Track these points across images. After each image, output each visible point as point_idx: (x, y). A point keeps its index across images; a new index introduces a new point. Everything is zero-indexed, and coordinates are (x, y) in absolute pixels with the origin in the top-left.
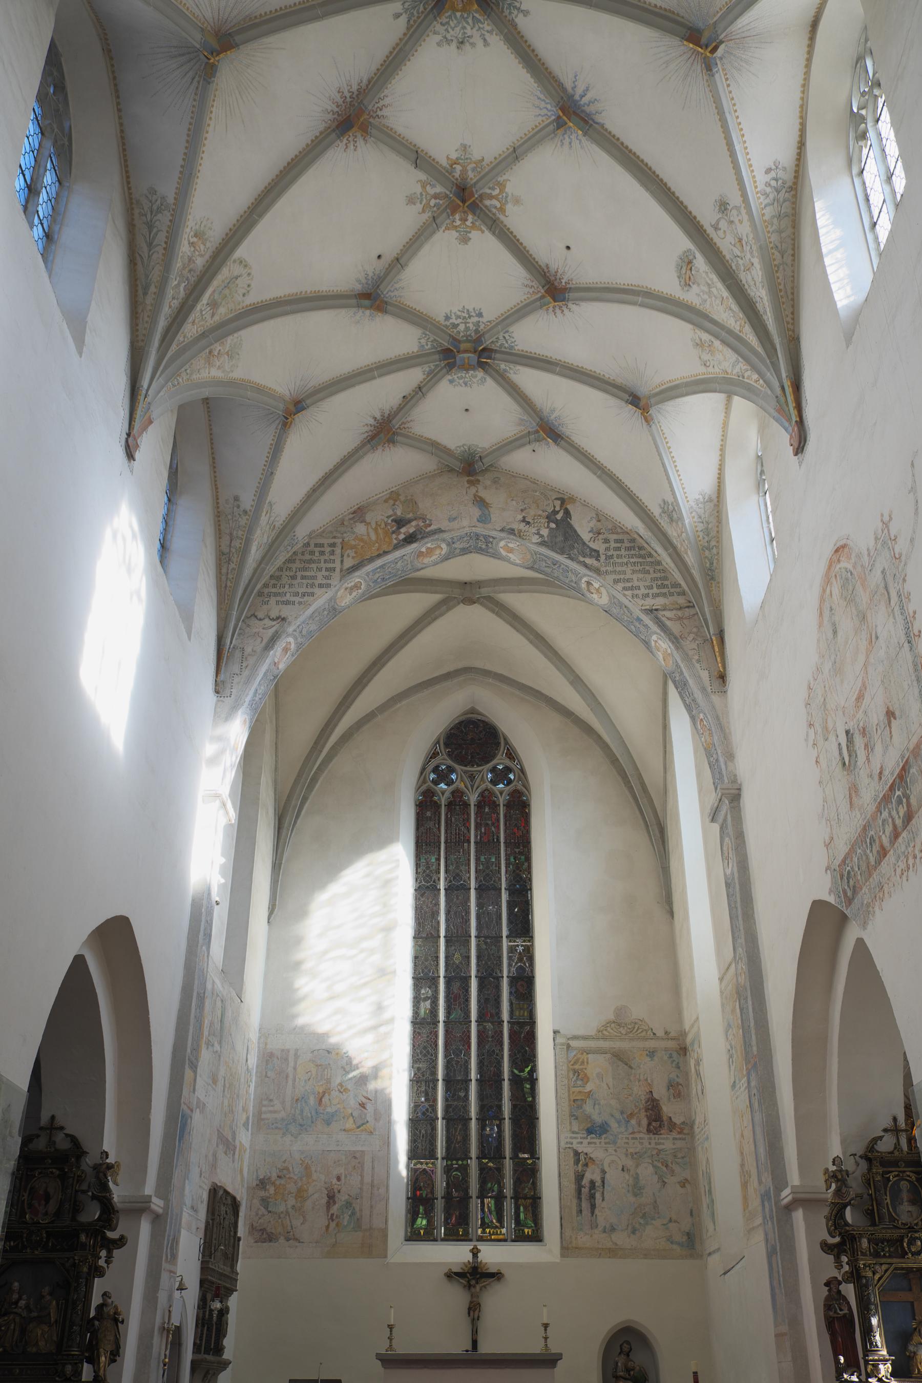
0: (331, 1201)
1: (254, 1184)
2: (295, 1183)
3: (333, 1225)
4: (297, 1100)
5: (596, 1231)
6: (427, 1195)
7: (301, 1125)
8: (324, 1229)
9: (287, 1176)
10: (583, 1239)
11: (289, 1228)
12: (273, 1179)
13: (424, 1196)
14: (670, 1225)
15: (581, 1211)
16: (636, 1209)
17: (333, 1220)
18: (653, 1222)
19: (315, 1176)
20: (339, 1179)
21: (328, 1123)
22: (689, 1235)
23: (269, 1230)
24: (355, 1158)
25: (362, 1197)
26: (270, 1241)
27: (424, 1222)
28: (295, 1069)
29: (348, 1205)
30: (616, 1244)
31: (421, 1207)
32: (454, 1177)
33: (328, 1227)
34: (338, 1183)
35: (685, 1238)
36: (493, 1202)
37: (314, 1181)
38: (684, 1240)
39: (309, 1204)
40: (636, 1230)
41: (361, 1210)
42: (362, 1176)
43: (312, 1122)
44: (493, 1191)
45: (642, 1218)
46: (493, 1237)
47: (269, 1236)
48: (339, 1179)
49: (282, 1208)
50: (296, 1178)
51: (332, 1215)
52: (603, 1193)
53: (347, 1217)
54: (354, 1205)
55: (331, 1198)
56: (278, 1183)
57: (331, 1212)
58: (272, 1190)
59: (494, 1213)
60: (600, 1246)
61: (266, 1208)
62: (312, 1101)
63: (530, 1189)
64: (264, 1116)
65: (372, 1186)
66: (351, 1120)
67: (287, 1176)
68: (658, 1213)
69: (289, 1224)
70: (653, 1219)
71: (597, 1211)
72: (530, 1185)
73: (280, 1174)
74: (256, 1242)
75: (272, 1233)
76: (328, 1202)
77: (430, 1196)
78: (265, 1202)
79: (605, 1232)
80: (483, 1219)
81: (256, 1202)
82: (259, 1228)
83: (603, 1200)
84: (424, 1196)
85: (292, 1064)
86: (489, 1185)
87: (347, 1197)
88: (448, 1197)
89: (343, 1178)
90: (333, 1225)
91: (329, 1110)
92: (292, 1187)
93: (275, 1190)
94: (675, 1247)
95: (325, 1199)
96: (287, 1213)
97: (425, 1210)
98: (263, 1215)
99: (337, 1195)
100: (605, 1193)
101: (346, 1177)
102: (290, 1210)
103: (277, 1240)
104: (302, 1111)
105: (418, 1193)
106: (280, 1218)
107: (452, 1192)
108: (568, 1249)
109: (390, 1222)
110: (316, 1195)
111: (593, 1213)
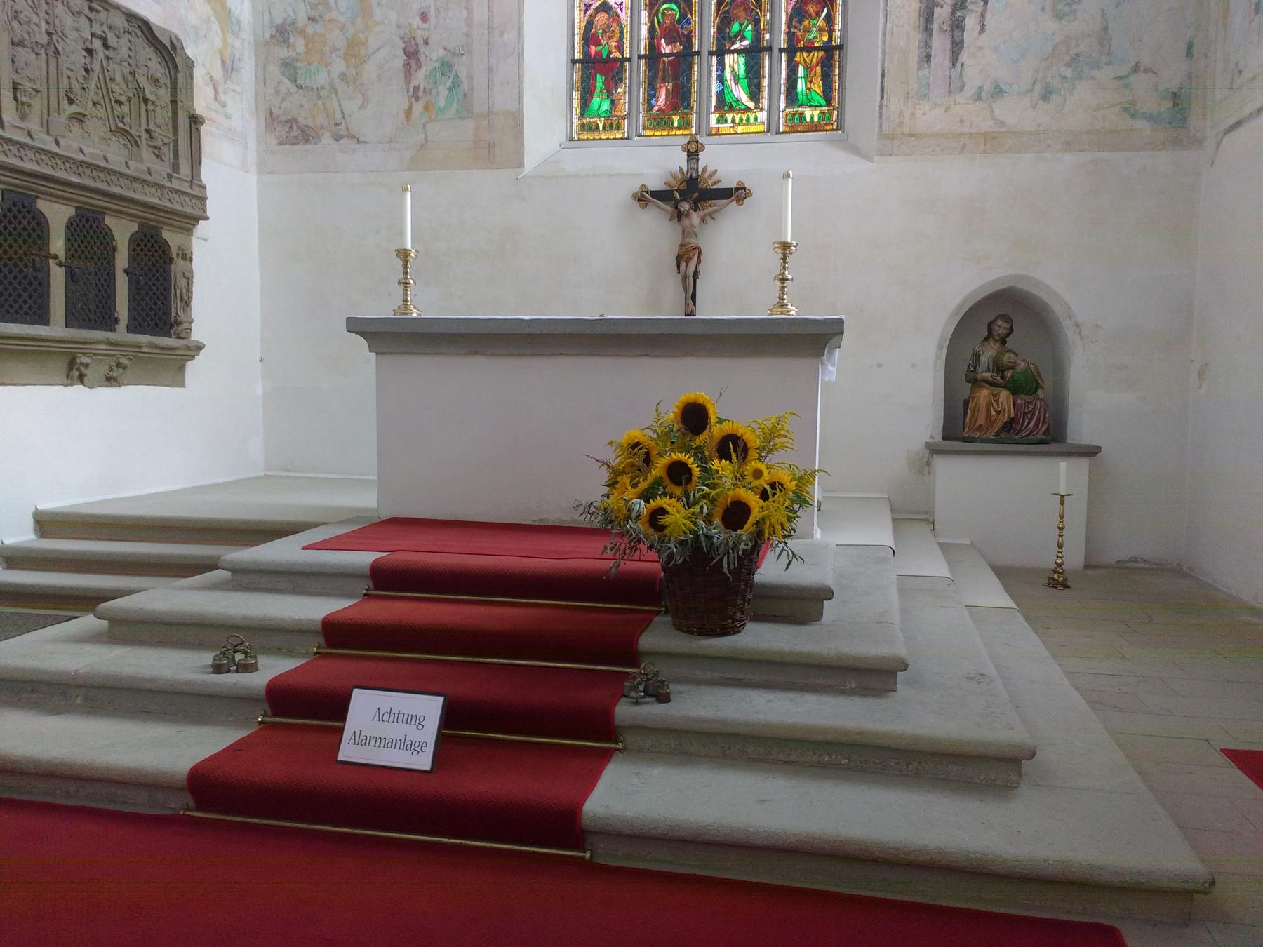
0: (413, 62)
1: (267, 36)
2: (343, 28)
3: (418, 108)
5: (960, 98)
6: (610, 53)
8: (402, 115)
9: (327, 17)
10: (930, 117)
11: (338, 116)
12: (300, 24)
13: (604, 55)
14: (1133, 78)
15: (928, 57)
16: (1055, 47)
17: (417, 99)
18: (1095, 73)
19: (378, 14)
20: (424, 17)
22: (1178, 100)
25: (471, 52)
26: (307, 141)
27: (606, 105)
29: (445, 67)
30: (1002, 123)
31: (599, 78)
32: (663, 14)
33: (409, 112)
34: (424, 26)
35: (1168, 104)
36: (742, 60)
37: (377, 24)
38: (1163, 109)
39: (370, 70)
40: (1051, 93)
41: (470, 77)
42: (469, 10)
44: (743, 38)
45: (1068, 65)
46: (740, 129)
47: (303, 131)
48: (424, 17)
49: (321, 79)
50: (342, 19)
52: (983, 16)
53: (443, 92)
54: (456, 68)
55: (412, 55)
56: (310, 30)
57: (414, 83)
58: (300, 44)
59: (745, 83)
60: (966, 129)
61: (294, 80)
63: (820, 30)
65: (490, 28)
67: (327, 17)
68: (1109, 54)
69: (338, 109)
70: (1096, 66)
71: (964, 57)
72: (821, 22)
73: (312, 14)
74: (280, 144)
75: (309, 127)
76: (407, 65)
77: (616, 54)
78: (289, 68)
79: (978, 98)
80: (720, 95)
81: (274, 70)
83: (982, 30)
84: (604, 55)
86: (736, 27)
87: (441, 52)
88: (653, 55)
89: (432, 15)
90: (418, 108)
92: (337, 39)
93: (306, 46)
94: (1140, 124)
95: (401, 59)
96: (333, 89)
97: (606, 83)
98: (289, 94)
99: (423, 49)
100: (988, 16)
101: (438, 11)
102: (337, 81)
103: (317, 138)
105: (593, 49)
106: (320, 97)
107: (660, 45)
108: (892, 138)
109: (528, 99)
110: (383, 53)
111: (955, 60)
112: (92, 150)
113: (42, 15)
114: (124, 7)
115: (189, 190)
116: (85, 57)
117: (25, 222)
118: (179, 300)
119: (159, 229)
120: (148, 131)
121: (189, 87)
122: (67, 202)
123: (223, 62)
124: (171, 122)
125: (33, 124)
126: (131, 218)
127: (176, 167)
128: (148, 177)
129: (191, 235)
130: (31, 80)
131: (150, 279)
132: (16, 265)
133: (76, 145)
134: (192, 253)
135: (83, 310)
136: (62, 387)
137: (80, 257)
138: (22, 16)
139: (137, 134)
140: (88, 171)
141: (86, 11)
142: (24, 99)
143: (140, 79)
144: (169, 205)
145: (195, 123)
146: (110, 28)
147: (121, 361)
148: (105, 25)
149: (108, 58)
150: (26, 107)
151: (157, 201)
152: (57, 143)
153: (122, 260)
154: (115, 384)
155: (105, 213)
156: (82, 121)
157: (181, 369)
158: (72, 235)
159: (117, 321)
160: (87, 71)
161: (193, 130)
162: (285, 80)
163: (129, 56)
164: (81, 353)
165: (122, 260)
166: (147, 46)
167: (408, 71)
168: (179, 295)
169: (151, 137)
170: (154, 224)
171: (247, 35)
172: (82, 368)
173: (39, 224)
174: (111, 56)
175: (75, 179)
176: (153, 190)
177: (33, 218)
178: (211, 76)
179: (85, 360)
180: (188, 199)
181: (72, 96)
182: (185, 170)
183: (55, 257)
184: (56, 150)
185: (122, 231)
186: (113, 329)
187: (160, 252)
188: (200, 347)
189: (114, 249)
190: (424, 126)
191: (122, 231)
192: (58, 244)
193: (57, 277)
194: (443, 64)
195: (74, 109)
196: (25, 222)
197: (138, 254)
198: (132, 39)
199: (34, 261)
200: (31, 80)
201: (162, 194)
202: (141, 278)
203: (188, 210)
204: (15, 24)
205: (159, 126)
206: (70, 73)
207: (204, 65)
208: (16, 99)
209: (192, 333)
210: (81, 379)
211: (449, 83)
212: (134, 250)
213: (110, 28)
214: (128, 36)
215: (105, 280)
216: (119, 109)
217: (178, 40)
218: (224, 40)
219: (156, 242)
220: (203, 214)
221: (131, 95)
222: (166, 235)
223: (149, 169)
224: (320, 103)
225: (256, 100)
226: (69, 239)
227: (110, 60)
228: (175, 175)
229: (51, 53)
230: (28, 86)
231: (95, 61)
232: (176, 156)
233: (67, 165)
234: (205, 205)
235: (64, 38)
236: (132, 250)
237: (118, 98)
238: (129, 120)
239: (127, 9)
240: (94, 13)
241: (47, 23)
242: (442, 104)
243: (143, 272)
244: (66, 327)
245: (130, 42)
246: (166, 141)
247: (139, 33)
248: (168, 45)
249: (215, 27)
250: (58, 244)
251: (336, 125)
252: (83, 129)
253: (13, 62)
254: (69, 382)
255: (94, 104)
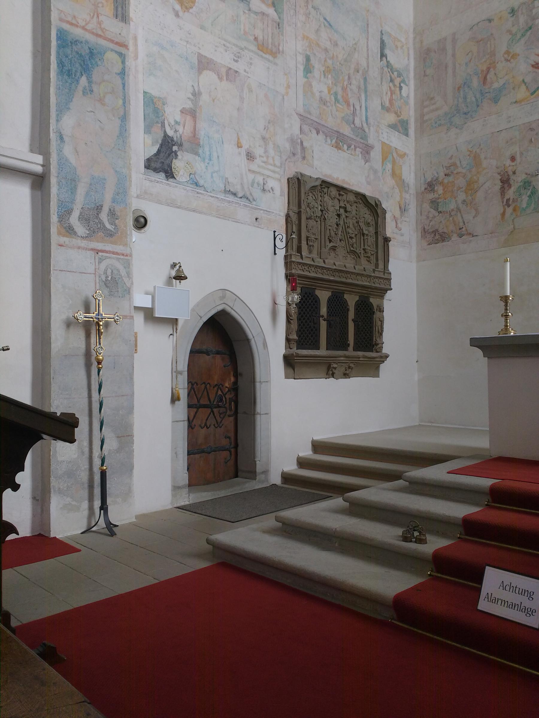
0: (506, 185)
1: (423, 189)
2: (464, 176)
3: (509, 210)
4: (459, 88)
7: (465, 114)
8: (499, 217)
9: (455, 172)
11: (461, 224)
12: (440, 179)
17: (509, 206)
20: (513, 159)
21: (496, 100)
23: (441, 231)
24: (532, 129)
26: (443, 241)
28: (454, 55)
29: (527, 184)
33: (503, 214)
34: (513, 164)
39: (480, 194)
43: (478, 106)
47: (441, 236)
48: (513, 159)
50: (464, 171)
51: (508, 200)
53: (525, 198)
54: (534, 183)
55: (505, 182)
56: (446, 181)
57: (507, 197)
58: (440, 190)
61: (436, 209)
62: (475, 83)
64: (426, 118)
66: (523, 87)
69: (461, 220)
73: (447, 172)
74: (429, 244)
75: (444, 233)
78: (434, 204)
81: (426, 206)
82: (431, 230)
85: (450, 52)
87: (524, 176)
91: (496, 85)
92: (461, 182)
93: (444, 190)
96: (459, 210)
98: (434, 217)
99: (512, 177)
101: (522, 154)
102: (461, 206)
104: (465, 98)
106: (451, 216)
112: (339, 263)
113: (319, 203)
114: (353, 190)
115: (383, 276)
116: (337, 218)
117: (310, 301)
118: (377, 332)
119: (368, 298)
120: (364, 249)
121: (384, 224)
122: (327, 290)
123: (400, 207)
124: (375, 242)
125: (314, 255)
126: (355, 294)
127: (377, 266)
128: (364, 273)
129: (384, 299)
130: (314, 234)
131: (364, 323)
132: (306, 322)
133: (332, 262)
134: (383, 308)
135: (334, 341)
136: (325, 379)
137: (333, 315)
138: (311, 205)
139: (359, 252)
140: (337, 274)
141: (338, 196)
142: (311, 244)
143: (361, 224)
144: (373, 285)
145: (387, 241)
146: (348, 202)
147: (350, 365)
148: (346, 201)
149: (347, 217)
150: (312, 247)
151: (368, 284)
152: (324, 262)
153: (351, 315)
154: (348, 377)
155: (344, 293)
156: (335, 250)
157: (378, 368)
158: (330, 305)
159: (349, 345)
160: (337, 225)
161: (386, 245)
162: (432, 210)
163: (356, 214)
164: (333, 362)
165: (351, 315)
166: (364, 207)
167: (503, 191)
168: (377, 330)
169: (365, 252)
170: (366, 295)
171: (412, 191)
172: (333, 370)
173: (316, 302)
174: (348, 216)
175: (332, 278)
176: (366, 279)
177: (314, 299)
178: (394, 216)
179: (335, 366)
180: (382, 281)
181: (331, 238)
182: (381, 266)
183: (323, 316)
184: (324, 265)
185: (351, 300)
186: (346, 350)
187: (369, 309)
188: (387, 356)
189: (348, 310)
190: (513, 220)
191: (351, 300)
192: (324, 311)
193: (323, 325)
194: (525, 183)
195: (332, 244)
196: (310, 301)
197: (359, 311)
198: (357, 205)
199: (314, 319)
200: (314, 234)
201: (370, 280)
202: (360, 323)
203: (382, 286)
204: (308, 209)
205: (369, 246)
206: (330, 227)
207: (391, 211)
208: (307, 244)
209: (383, 349)
210: (333, 375)
211: (529, 193)
212: (357, 309)
213: (348, 202)
214: (355, 204)
215: (344, 325)
216: (351, 241)
217: (379, 201)
218: (401, 197)
219: (367, 304)
220: (390, 288)
221: (357, 233)
222: (372, 300)
223: (364, 268)
224: (451, 219)
225: (417, 222)
226: (329, 307)
227: (348, 218)
228: (376, 269)
229: (322, 220)
230: (313, 237)
231: (341, 219)
232: (377, 260)
233: (328, 271)
234: (391, 282)
235: (328, 212)
236: (356, 309)
237: (351, 236)
238: (355, 245)
239: (356, 191)
240: (341, 196)
241: (321, 206)
242: (524, 205)
243: (361, 320)
244: (327, 350)
245: (357, 207)
246: (372, 253)
247: (361, 202)
248: (374, 204)
249: (397, 190)
250: (324, 311)
251: (460, 229)
252: (335, 253)
253: (307, 227)
254: (328, 376)
255: (340, 240)
